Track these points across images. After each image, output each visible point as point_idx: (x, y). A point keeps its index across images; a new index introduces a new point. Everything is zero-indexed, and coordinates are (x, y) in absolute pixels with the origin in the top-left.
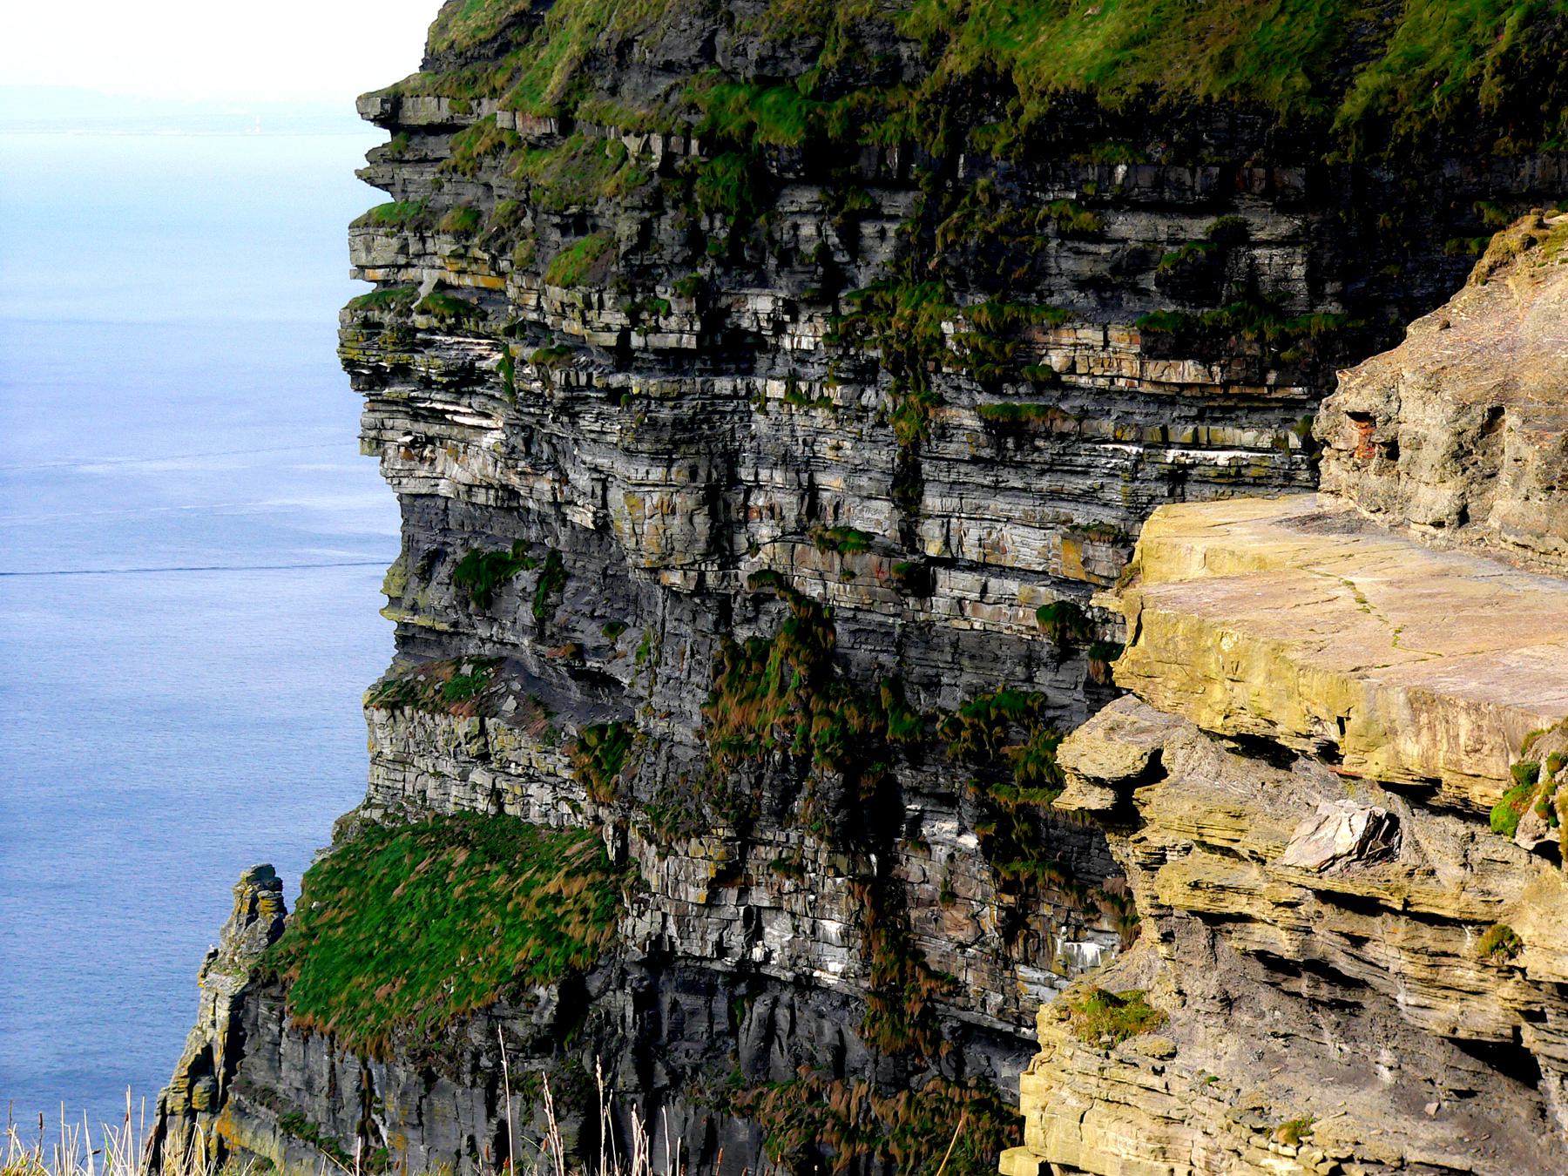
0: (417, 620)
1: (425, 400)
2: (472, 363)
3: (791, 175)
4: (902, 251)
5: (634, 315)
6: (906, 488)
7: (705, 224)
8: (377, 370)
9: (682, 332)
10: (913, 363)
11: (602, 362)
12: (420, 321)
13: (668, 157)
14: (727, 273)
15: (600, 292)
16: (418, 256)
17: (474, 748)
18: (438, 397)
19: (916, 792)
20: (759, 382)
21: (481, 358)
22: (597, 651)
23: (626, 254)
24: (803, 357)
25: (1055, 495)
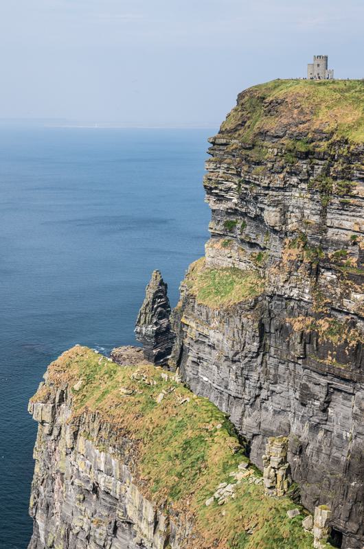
0: (216, 232)
6: (323, 213)
10: (325, 191)
17: (229, 255)
19: (323, 268)
22: (254, 239)
25: (353, 216)
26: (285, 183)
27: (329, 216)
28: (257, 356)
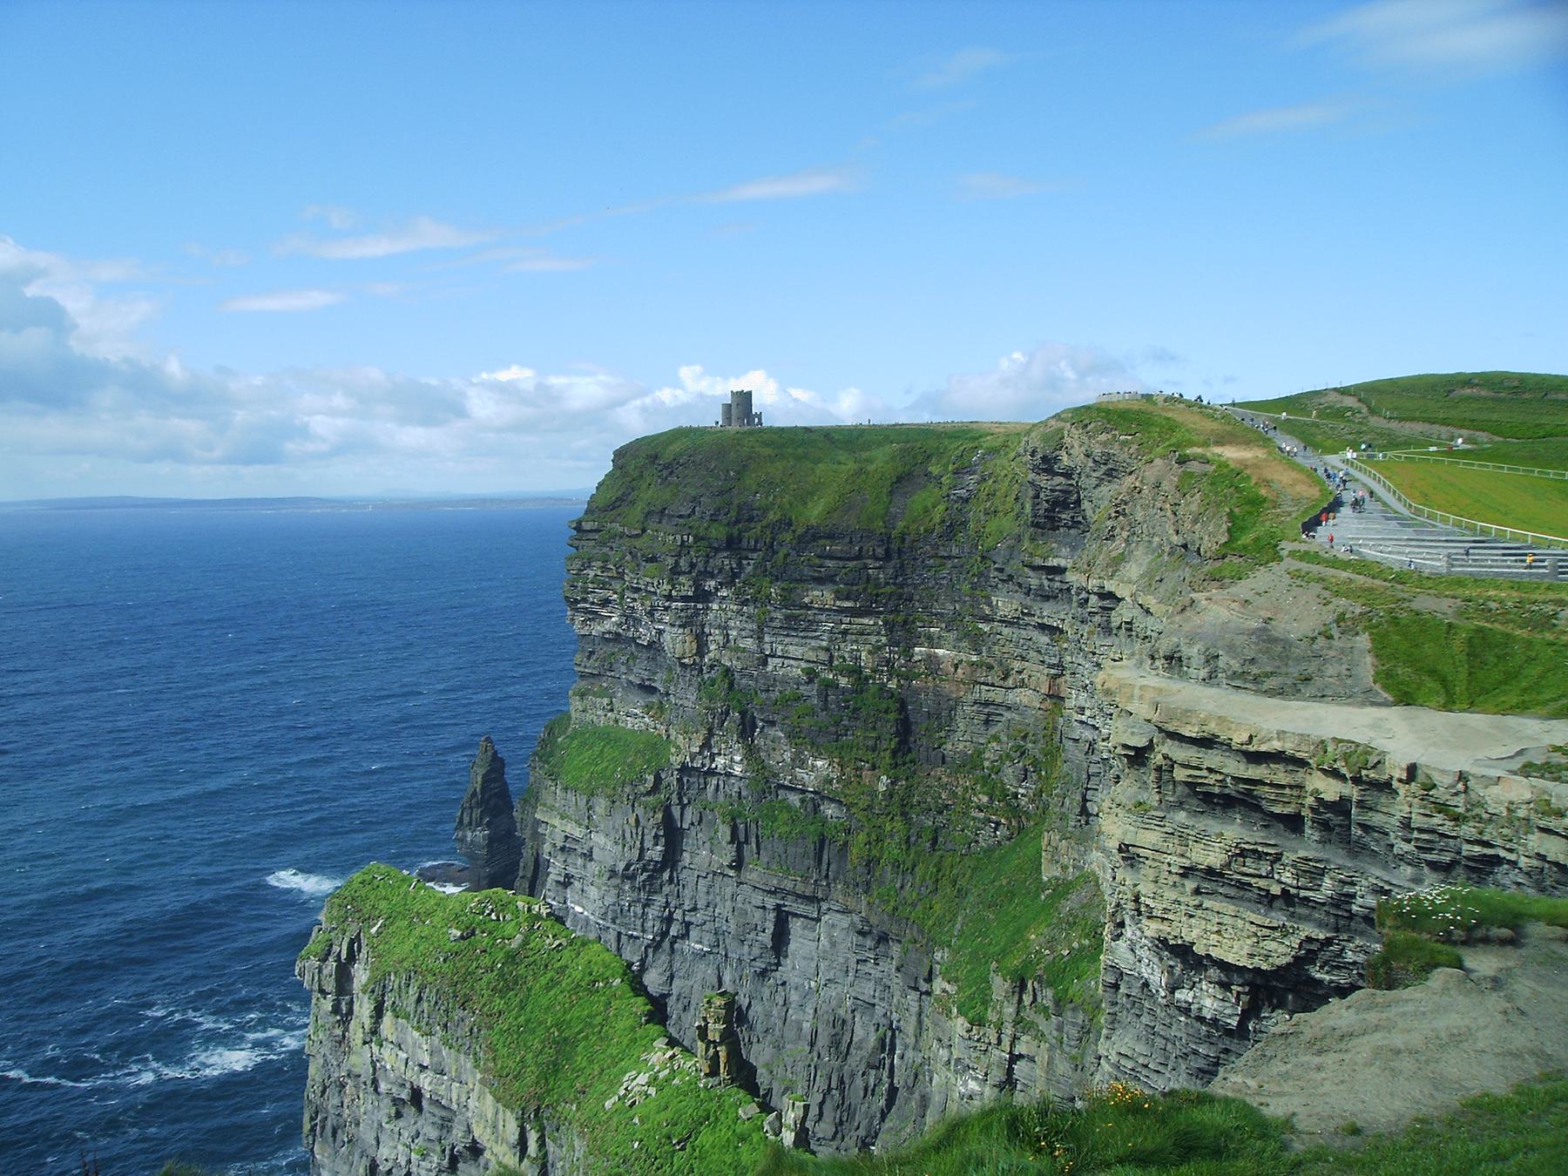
4: (755, 568)
27: (767, 639)
28: (662, 870)
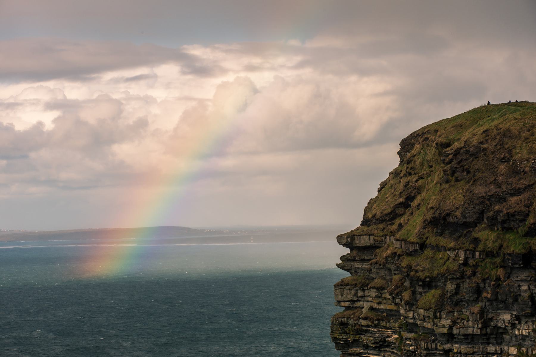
1: (365, 354)
2: (385, 340)
3: (517, 266)
5: (454, 322)
7: (482, 285)
8: (346, 341)
9: (474, 327)
11: (441, 339)
12: (364, 322)
13: (466, 259)
14: (491, 304)
15: (440, 312)
16: (362, 297)
18: (371, 352)
20: (506, 348)
21: (388, 337)
23: (450, 297)
24: (524, 338)
26: (485, 324)
